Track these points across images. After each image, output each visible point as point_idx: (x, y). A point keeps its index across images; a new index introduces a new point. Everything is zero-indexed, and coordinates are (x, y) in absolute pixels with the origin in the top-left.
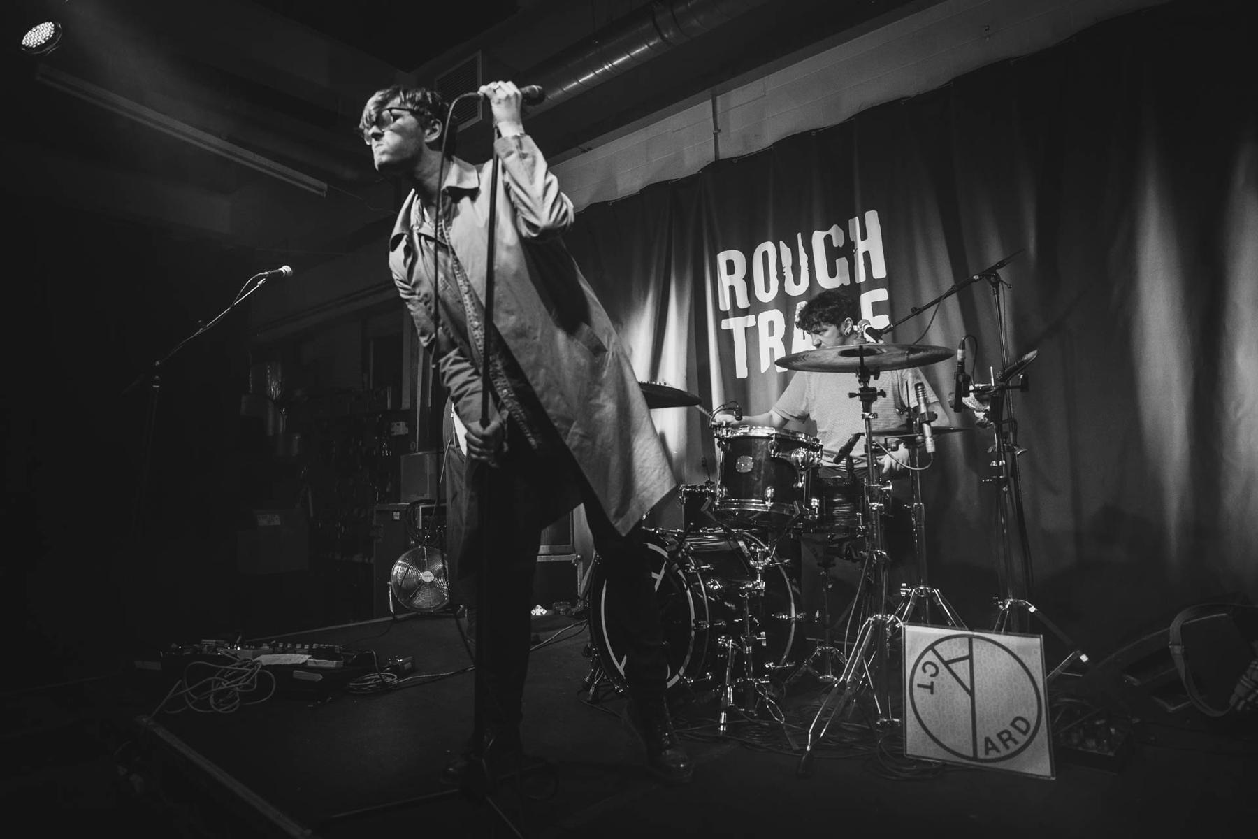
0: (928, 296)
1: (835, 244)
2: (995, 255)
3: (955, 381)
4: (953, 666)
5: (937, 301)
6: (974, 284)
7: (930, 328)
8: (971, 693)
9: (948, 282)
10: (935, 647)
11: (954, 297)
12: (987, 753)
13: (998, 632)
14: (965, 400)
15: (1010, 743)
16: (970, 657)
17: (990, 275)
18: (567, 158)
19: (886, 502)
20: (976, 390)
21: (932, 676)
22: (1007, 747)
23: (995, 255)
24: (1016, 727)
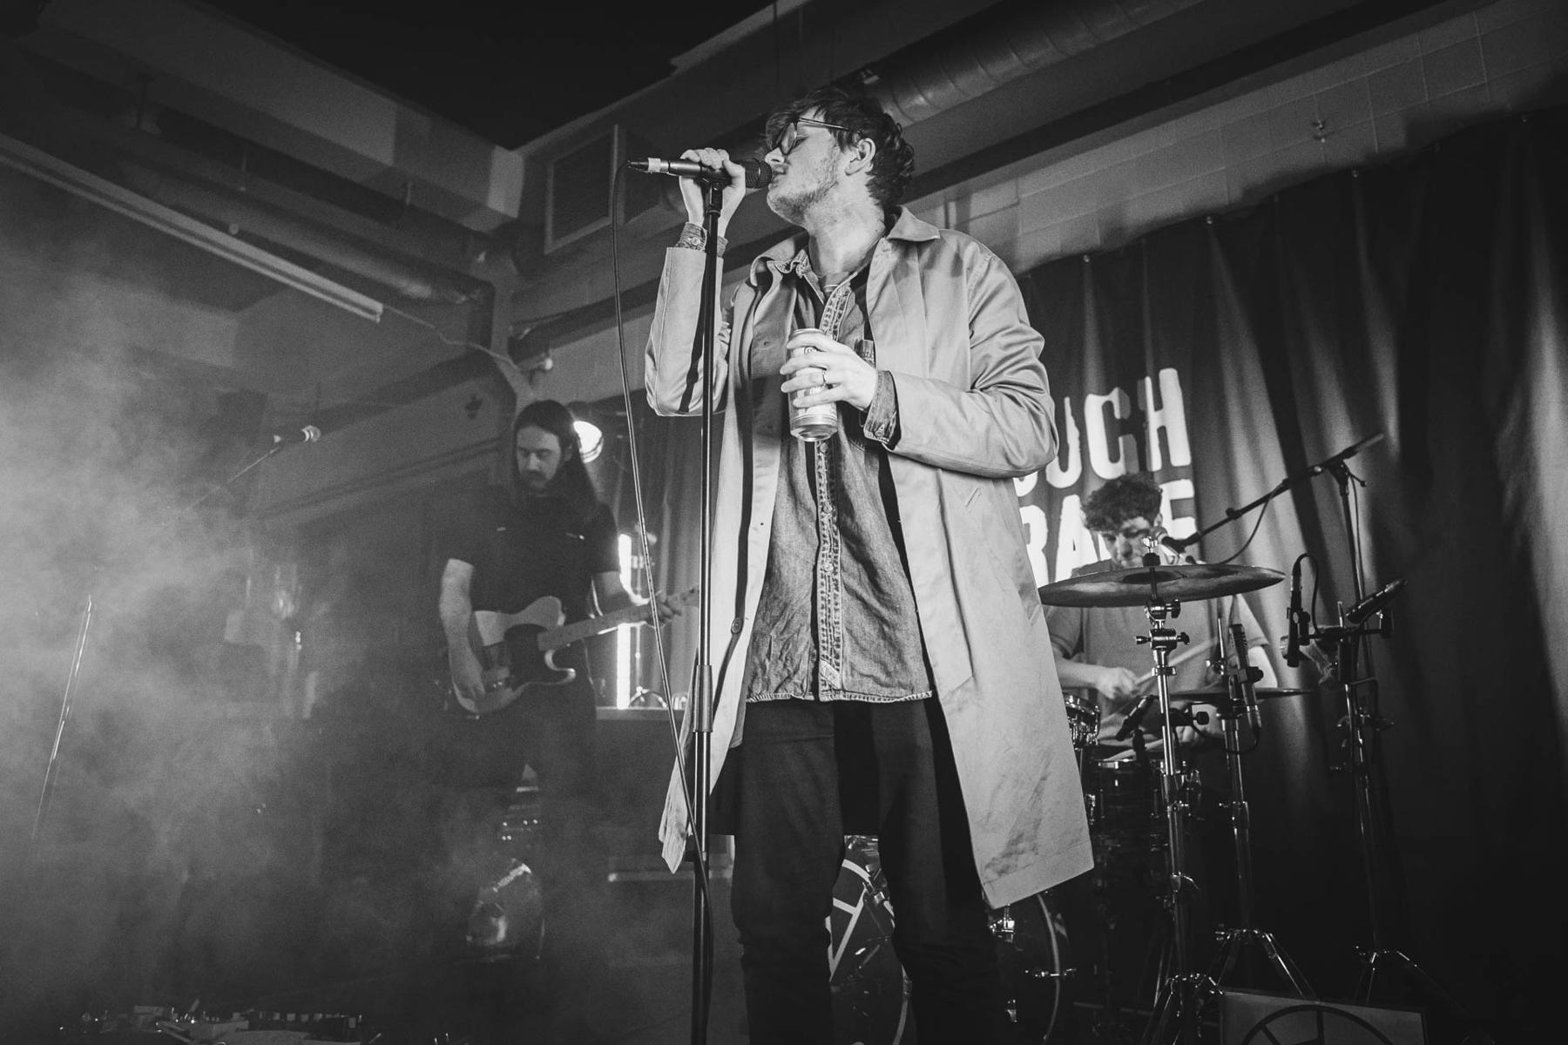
0: (1249, 492)
1: (1117, 415)
2: (1341, 438)
3: (1288, 621)
5: (1265, 500)
6: (1313, 478)
7: (1252, 542)
9: (1277, 473)
10: (1268, 1026)
11: (1287, 495)
13: (1360, 1002)
14: (1302, 648)
19: (1192, 801)
23: (1341, 438)
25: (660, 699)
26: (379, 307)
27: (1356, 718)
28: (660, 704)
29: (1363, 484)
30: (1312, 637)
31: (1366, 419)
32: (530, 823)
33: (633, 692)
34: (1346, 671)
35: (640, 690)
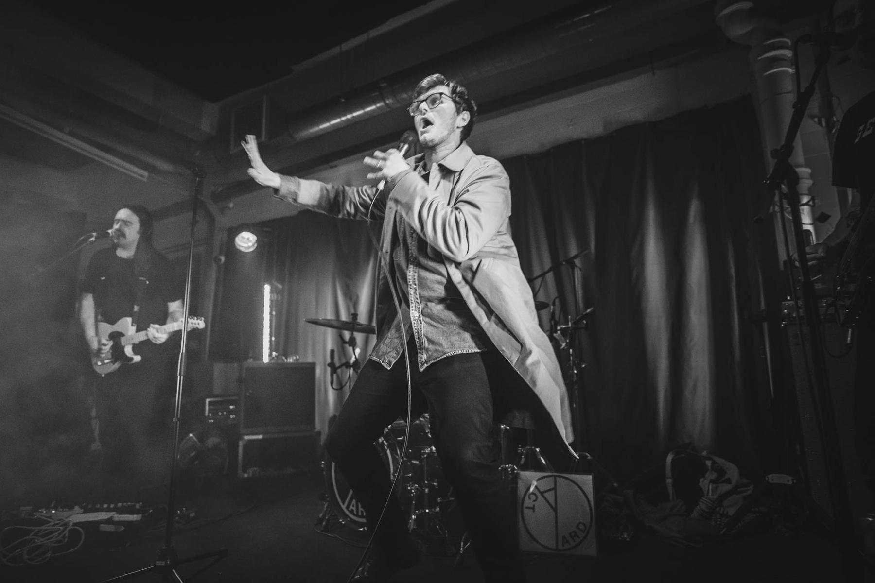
2: (573, 251)
3: (549, 324)
4: (546, 495)
8: (555, 509)
9: (548, 265)
12: (563, 546)
13: (571, 473)
14: (555, 335)
15: (576, 538)
16: (555, 489)
17: (571, 263)
18: (320, 170)
20: (561, 330)
21: (534, 501)
22: (574, 541)
23: (573, 251)
24: (579, 529)
25: (284, 358)
26: (146, 174)
27: (574, 362)
28: (283, 360)
29: (581, 270)
30: (559, 330)
31: (583, 244)
32: (222, 413)
33: (270, 355)
34: (570, 345)
35: (274, 354)
